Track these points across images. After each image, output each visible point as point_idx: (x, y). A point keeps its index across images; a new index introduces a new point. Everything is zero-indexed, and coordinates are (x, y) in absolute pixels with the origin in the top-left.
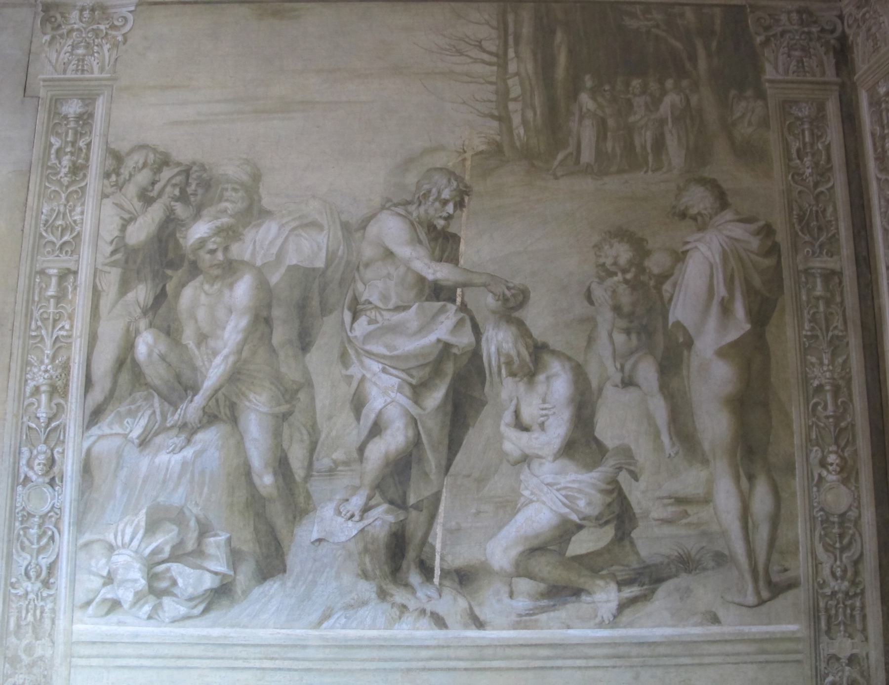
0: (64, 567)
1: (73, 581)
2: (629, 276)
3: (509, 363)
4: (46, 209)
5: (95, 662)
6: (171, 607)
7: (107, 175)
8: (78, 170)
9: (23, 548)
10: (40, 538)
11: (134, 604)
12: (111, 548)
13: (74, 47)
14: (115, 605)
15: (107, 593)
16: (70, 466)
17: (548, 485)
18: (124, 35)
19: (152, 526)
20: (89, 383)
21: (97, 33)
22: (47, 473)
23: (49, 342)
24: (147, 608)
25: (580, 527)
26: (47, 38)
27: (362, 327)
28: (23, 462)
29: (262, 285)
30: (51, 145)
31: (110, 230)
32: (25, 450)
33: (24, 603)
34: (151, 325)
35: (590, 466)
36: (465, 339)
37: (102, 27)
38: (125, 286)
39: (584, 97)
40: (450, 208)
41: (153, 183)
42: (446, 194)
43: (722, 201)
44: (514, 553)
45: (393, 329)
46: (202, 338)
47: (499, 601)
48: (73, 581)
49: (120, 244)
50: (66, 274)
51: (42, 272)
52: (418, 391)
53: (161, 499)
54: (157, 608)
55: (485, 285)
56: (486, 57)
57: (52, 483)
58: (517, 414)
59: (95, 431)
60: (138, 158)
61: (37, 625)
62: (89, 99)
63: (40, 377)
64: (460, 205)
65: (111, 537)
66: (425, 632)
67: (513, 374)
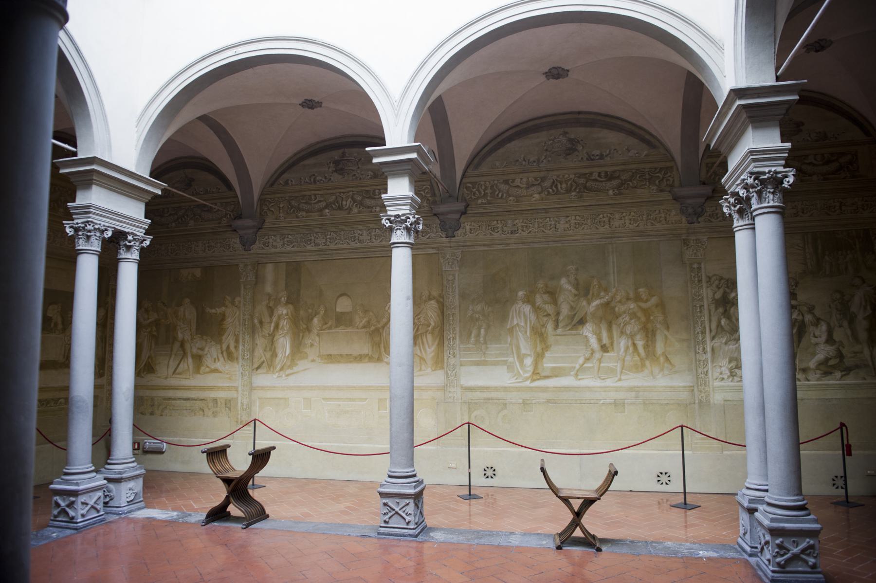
1: (712, 375)
2: (840, 301)
3: (811, 323)
4: (693, 291)
5: (720, 391)
7: (707, 282)
8: (700, 281)
9: (700, 367)
10: (703, 365)
11: (728, 378)
12: (721, 367)
13: (693, 250)
14: (723, 379)
15: (721, 376)
16: (709, 349)
17: (823, 350)
18: (706, 247)
19: (730, 362)
20: (711, 331)
21: (698, 246)
22: (703, 351)
23: (699, 322)
24: (731, 379)
25: (831, 359)
26: (686, 248)
28: (697, 349)
30: (692, 275)
31: (711, 295)
32: (697, 346)
33: (701, 379)
34: (724, 317)
35: (832, 345)
36: (800, 318)
37: (700, 244)
38: (716, 309)
39: (827, 258)
40: (794, 287)
41: (720, 284)
42: (793, 284)
43: (864, 281)
44: (816, 364)
47: (813, 375)
48: (712, 375)
49: (714, 299)
50: (701, 306)
51: (695, 306)
53: (731, 356)
54: (733, 379)
55: (804, 305)
56: (800, 248)
57: (705, 353)
58: (814, 334)
59: (714, 341)
60: (715, 278)
61: (705, 384)
62: (699, 263)
63: (698, 330)
64: (796, 286)
65: (720, 364)
67: (812, 325)
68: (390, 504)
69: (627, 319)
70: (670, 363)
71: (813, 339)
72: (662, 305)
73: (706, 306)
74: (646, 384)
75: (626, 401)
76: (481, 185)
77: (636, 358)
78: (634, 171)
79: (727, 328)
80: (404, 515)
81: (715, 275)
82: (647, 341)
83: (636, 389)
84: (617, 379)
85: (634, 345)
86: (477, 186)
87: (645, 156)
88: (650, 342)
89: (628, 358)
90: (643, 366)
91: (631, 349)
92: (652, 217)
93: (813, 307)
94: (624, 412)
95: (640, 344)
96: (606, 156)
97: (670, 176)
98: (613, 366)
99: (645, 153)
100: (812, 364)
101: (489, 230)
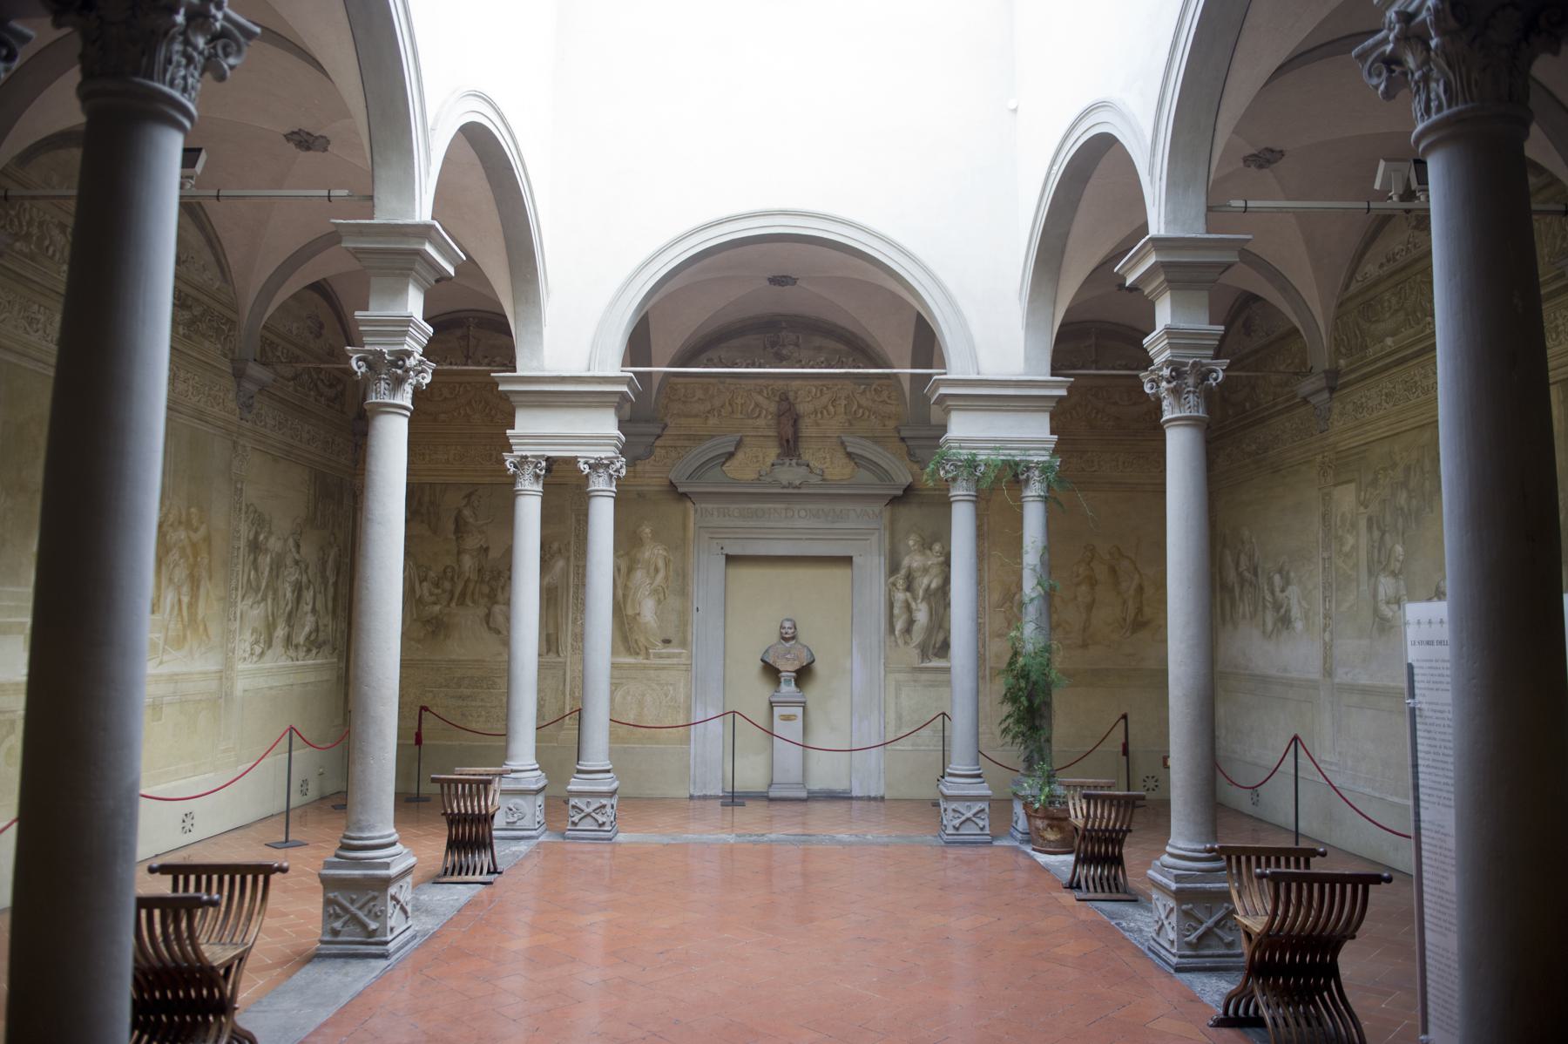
0: (237, 648)
6: (255, 659)
8: (240, 509)
14: (245, 659)
19: (252, 634)
20: (242, 588)
27: (286, 573)
29: (271, 558)
31: (246, 535)
35: (314, 615)
38: (249, 556)
45: (289, 574)
46: (262, 573)
50: (239, 548)
52: (293, 592)
62: (242, 482)
66: (289, 663)
68: (397, 896)
69: (177, 557)
70: (207, 636)
71: (305, 606)
72: (208, 539)
73: (242, 549)
74: (185, 669)
75: (165, 698)
76: (25, 210)
77: (180, 626)
78: (205, 307)
79: (254, 584)
80: (404, 904)
81: (252, 504)
82: (191, 598)
83: (176, 677)
84: (158, 660)
85: (180, 601)
86: (17, 208)
87: (218, 289)
88: (194, 600)
89: (172, 625)
90: (185, 637)
91: (176, 607)
92: (212, 392)
93: (307, 567)
94: (160, 719)
95: (185, 600)
96: (184, 262)
97: (233, 336)
98: (157, 638)
99: (218, 284)
100: (301, 640)
101: (23, 318)
